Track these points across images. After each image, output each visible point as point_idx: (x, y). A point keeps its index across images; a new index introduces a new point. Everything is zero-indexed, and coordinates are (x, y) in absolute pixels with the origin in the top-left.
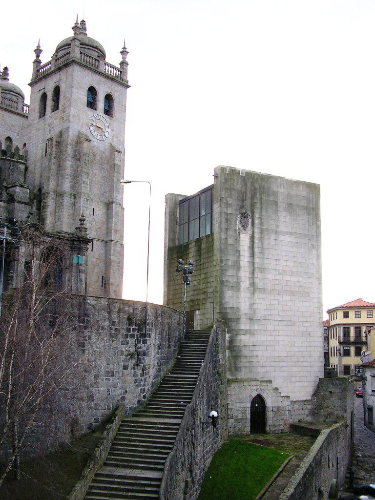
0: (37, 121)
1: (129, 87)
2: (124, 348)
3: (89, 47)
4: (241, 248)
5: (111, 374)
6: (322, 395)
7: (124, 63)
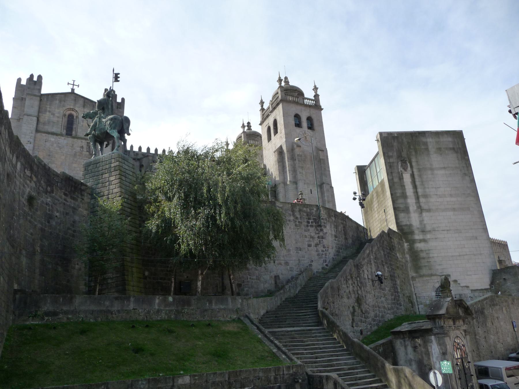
0: (267, 145)
1: (322, 109)
2: (307, 234)
3: (291, 91)
4: (405, 184)
5: (298, 249)
6: (498, 283)
7: (317, 96)
